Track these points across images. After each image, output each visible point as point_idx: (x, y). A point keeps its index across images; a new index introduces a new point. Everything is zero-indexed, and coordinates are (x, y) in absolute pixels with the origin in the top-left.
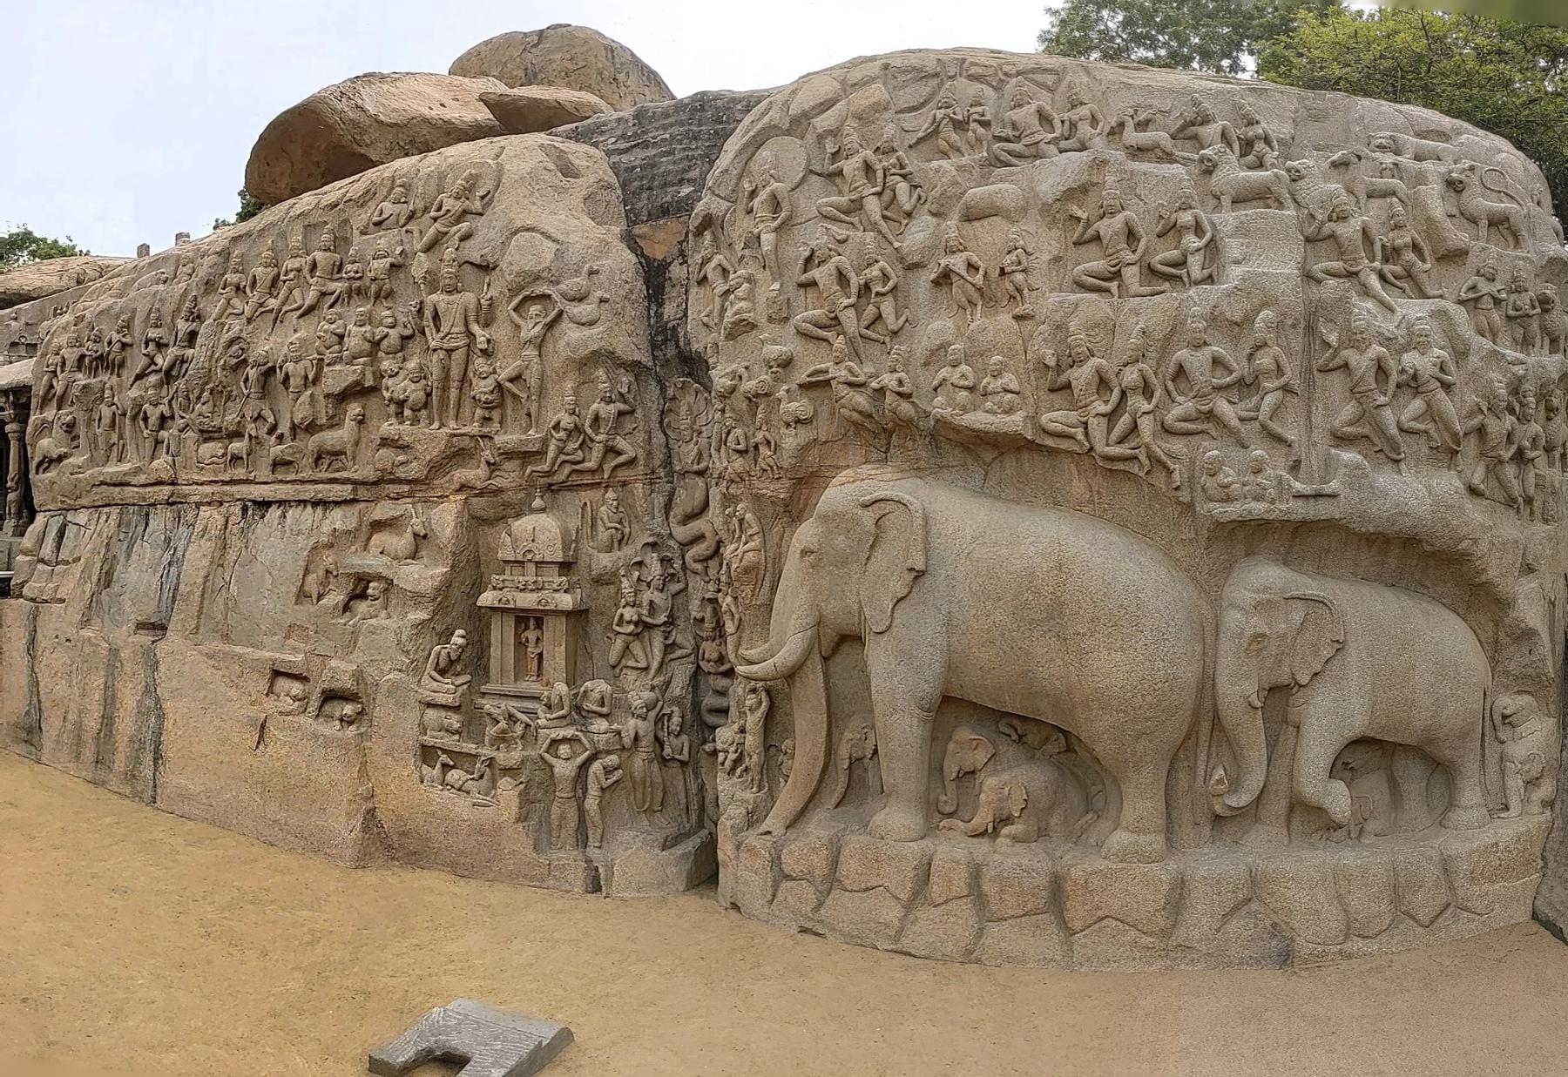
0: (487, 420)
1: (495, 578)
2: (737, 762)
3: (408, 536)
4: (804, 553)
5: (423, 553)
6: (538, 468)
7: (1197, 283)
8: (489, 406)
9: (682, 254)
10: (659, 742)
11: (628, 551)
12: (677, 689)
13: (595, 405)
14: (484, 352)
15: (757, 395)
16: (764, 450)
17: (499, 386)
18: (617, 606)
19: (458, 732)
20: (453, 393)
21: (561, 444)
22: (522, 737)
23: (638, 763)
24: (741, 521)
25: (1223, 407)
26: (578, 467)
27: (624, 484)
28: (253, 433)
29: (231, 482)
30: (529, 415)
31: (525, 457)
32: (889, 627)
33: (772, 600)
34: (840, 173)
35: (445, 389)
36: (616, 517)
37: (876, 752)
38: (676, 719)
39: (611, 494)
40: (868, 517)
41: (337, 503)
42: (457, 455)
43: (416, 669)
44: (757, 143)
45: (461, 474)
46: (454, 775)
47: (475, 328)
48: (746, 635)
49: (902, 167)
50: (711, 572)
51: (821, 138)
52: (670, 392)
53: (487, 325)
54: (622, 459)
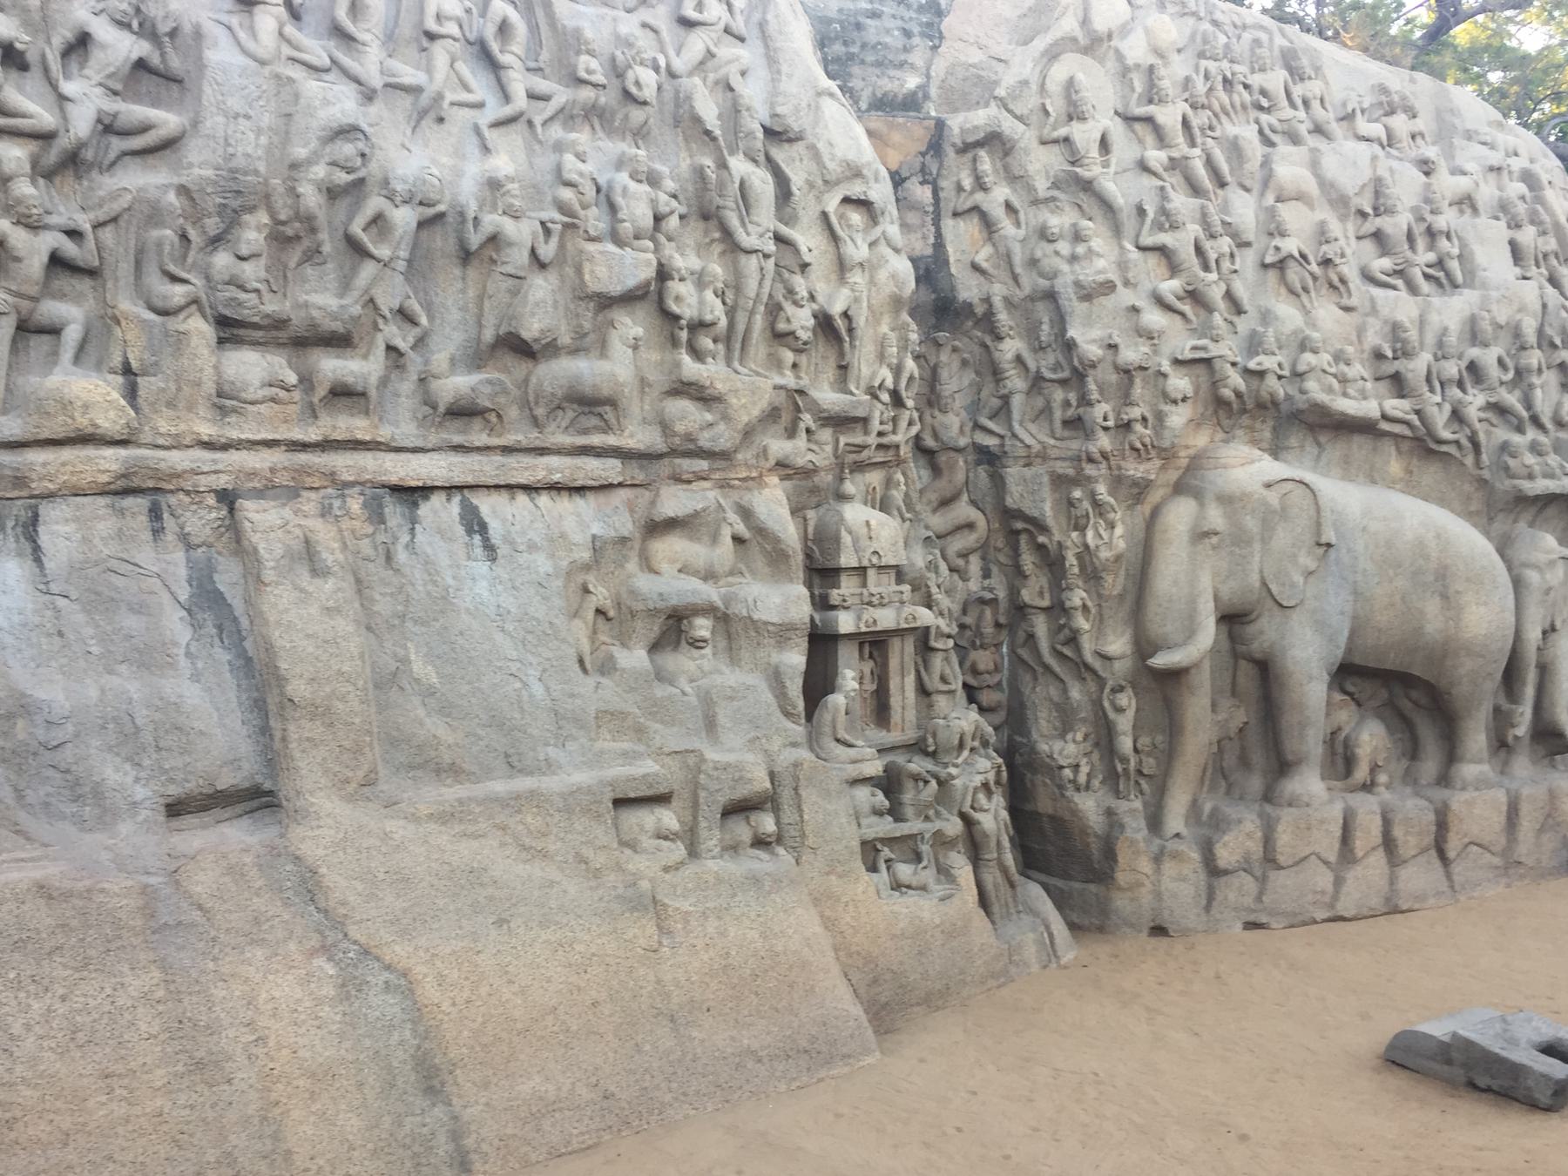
0: (795, 366)
4: (1207, 534)
6: (858, 439)
7: (1456, 286)
9: (923, 170)
14: (804, 266)
16: (1138, 427)
25: (1512, 399)
28: (402, 345)
29: (326, 445)
31: (840, 422)
34: (1149, 120)
35: (752, 313)
41: (580, 490)
44: (1052, 55)
46: (904, 871)
47: (785, 230)
49: (1211, 128)
51: (1125, 72)
53: (786, 224)
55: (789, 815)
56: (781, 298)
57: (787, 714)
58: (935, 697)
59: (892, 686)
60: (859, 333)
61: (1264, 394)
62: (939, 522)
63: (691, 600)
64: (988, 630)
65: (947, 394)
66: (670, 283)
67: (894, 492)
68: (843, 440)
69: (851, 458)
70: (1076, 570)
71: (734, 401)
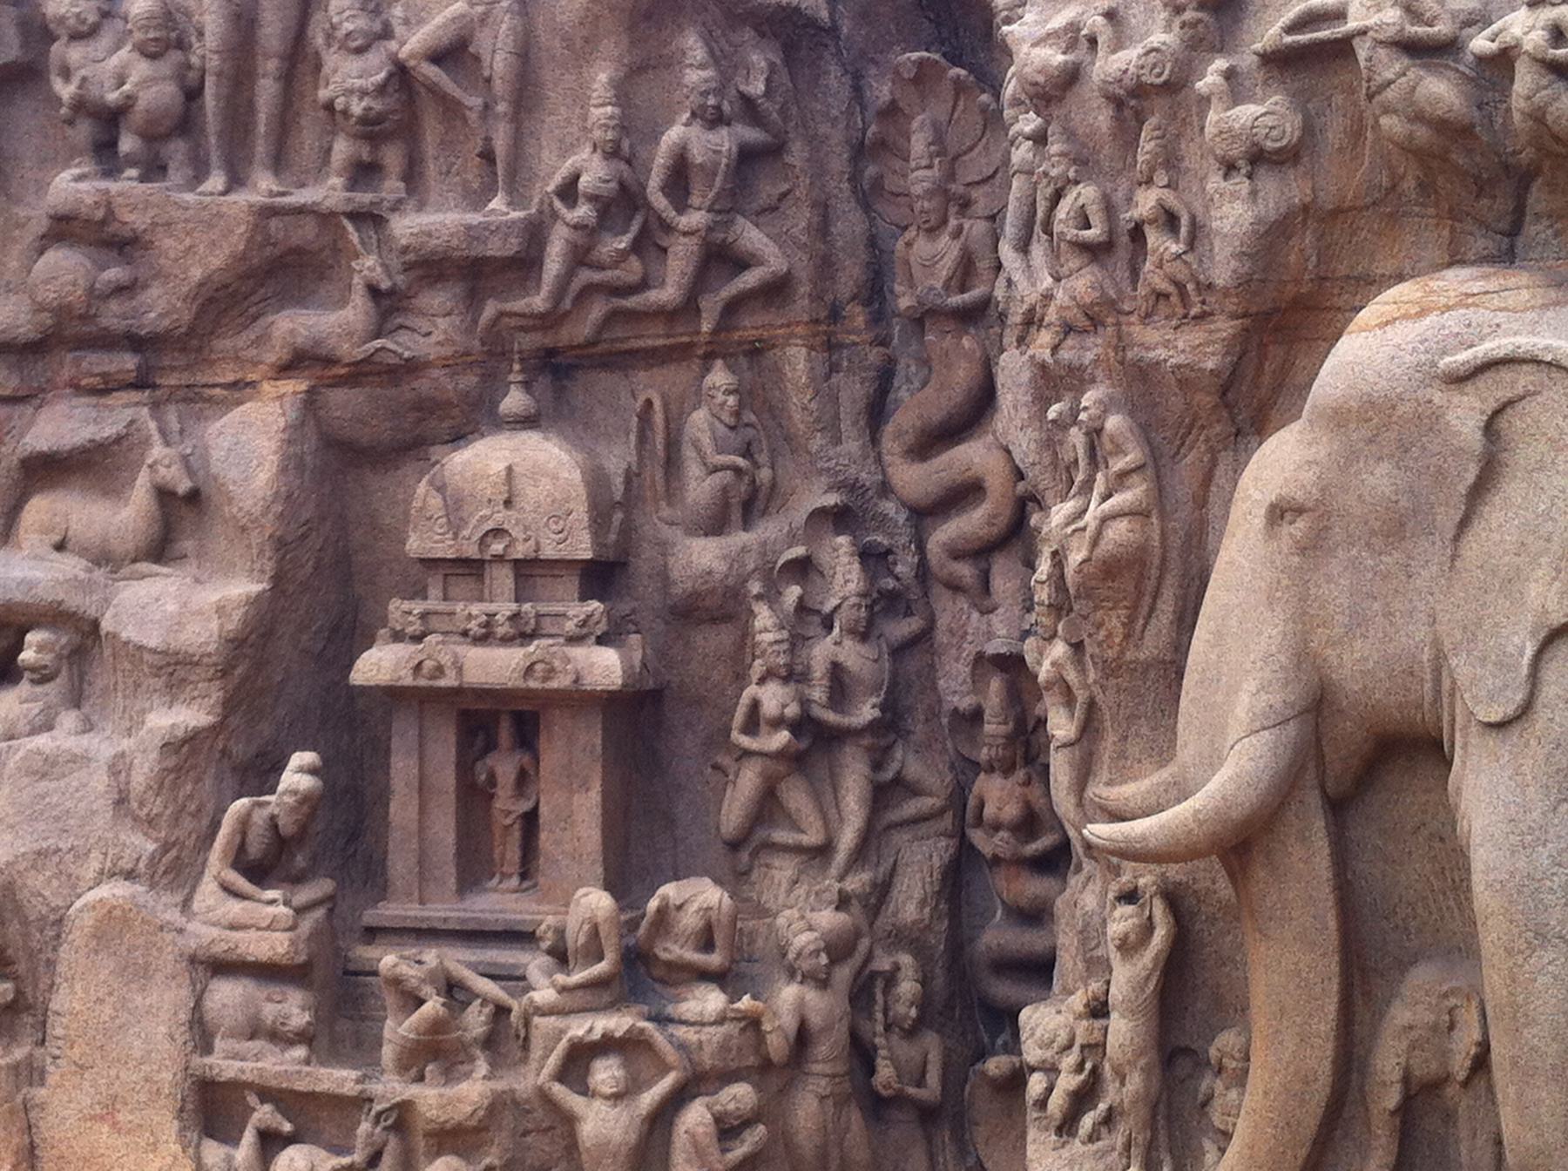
1: (398, 608)
2: (1083, 1098)
3: (140, 497)
4: (1279, 513)
5: (188, 545)
6: (518, 305)
8: (372, 130)
10: (862, 1054)
11: (769, 530)
12: (911, 900)
13: (674, 134)
15: (1140, 91)
17: (401, 74)
18: (741, 679)
19: (303, 1037)
20: (266, 91)
21: (578, 237)
22: (490, 1042)
23: (807, 1110)
24: (1095, 434)
26: (631, 302)
27: (755, 351)
30: (488, 156)
32: (1526, 709)
33: (1181, 648)
35: (240, 77)
36: (736, 440)
37: (1481, 1062)
38: (907, 987)
39: (719, 377)
40: (1464, 416)
42: (284, 265)
43: (176, 870)
45: (295, 324)
48: (1109, 743)
50: (1003, 582)
52: (882, 91)
54: (750, 279)
55: (61, 1001)
56: (320, 40)
57: (136, 819)
58: (744, 856)
59: (544, 810)
60: (498, 86)
61: (1517, 116)
62: (916, 478)
63: (18, 596)
64: (993, 727)
65: (917, 190)
66: (56, 48)
67: (700, 417)
68: (490, 309)
69: (529, 341)
70: (1043, 595)
71: (168, 242)
